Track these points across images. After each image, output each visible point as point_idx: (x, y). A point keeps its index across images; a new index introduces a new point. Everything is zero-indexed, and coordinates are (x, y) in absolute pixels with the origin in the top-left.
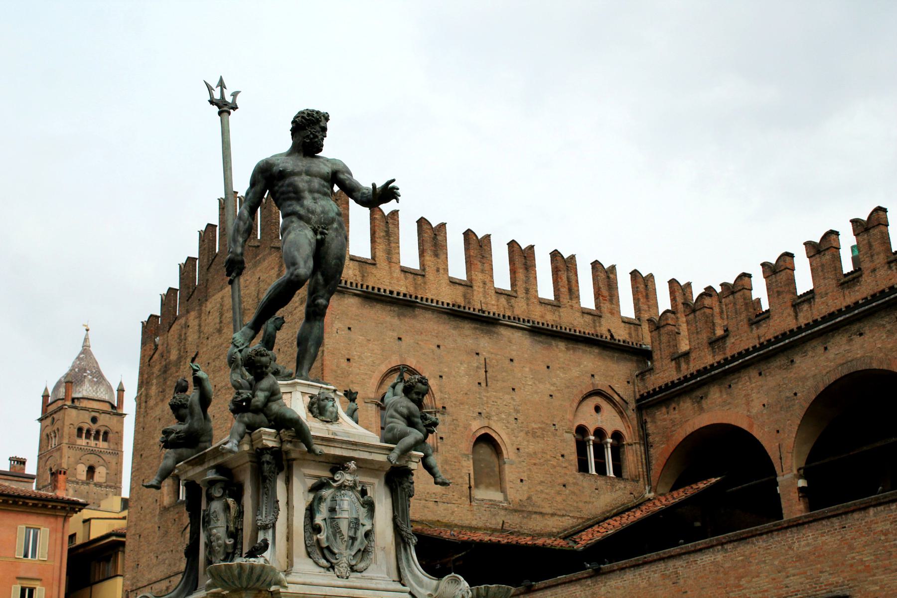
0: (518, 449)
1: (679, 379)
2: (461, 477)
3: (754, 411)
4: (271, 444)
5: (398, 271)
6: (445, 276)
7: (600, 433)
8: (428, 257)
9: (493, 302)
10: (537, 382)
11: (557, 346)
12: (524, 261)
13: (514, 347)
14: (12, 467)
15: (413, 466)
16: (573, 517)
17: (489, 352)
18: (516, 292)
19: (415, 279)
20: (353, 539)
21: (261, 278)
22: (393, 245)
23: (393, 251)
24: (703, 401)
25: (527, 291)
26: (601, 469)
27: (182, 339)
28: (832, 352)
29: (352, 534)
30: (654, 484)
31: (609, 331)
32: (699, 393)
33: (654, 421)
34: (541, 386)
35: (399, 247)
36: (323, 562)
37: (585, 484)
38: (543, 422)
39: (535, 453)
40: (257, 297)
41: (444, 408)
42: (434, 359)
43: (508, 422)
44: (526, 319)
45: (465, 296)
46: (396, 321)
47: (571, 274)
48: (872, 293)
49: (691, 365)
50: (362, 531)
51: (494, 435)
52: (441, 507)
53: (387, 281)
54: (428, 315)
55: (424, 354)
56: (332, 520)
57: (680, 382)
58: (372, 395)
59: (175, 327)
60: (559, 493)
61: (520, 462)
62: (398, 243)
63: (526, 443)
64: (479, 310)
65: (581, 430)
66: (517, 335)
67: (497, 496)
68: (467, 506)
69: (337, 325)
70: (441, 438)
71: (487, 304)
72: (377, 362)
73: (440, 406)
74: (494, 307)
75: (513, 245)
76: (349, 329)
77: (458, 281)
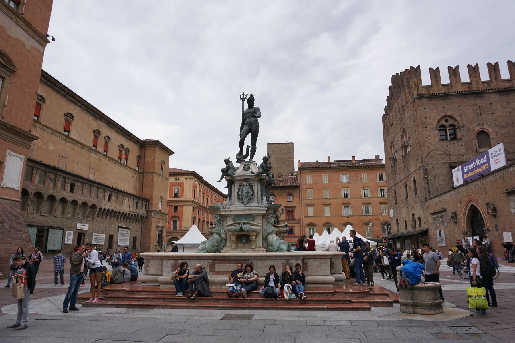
0: (496, 133)
2: (473, 146)
4: (228, 179)
5: (441, 86)
9: (481, 86)
10: (503, 109)
13: (492, 99)
14: (376, 158)
15: (264, 178)
19: (448, 87)
20: (247, 196)
22: (438, 78)
23: (439, 80)
25: (496, 79)
27: (389, 120)
29: (246, 195)
34: (505, 110)
35: (440, 78)
36: (241, 202)
38: (507, 122)
39: (504, 133)
41: (463, 125)
42: (458, 111)
43: (491, 125)
44: (497, 88)
45: (469, 87)
46: (442, 102)
50: (250, 195)
51: (485, 130)
56: (242, 193)
58: (436, 127)
59: (388, 117)
61: (497, 137)
62: (440, 77)
63: (500, 130)
64: (475, 91)
66: (493, 95)
69: (420, 108)
70: (463, 135)
71: (478, 87)
72: (436, 116)
73: (461, 125)
76: (425, 108)
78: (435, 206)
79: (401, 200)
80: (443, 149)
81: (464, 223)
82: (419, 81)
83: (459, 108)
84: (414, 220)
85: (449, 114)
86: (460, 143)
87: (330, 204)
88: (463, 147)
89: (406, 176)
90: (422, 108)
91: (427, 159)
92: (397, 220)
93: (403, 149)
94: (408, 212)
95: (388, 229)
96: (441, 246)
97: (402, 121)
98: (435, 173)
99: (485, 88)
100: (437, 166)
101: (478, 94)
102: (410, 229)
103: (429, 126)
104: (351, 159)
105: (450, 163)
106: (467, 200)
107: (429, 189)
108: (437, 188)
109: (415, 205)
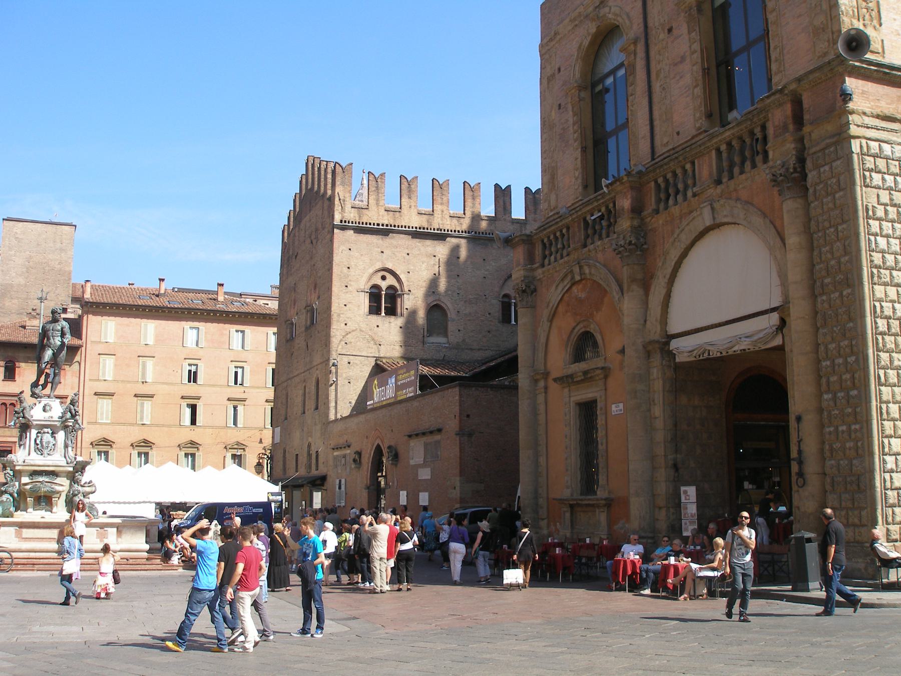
6: (416, 210)
9: (448, 223)
11: (492, 246)
12: (471, 193)
19: (394, 215)
22: (380, 195)
39: (470, 314)
41: (409, 291)
42: (404, 262)
45: (428, 221)
46: (380, 242)
47: (507, 199)
51: (442, 304)
53: (375, 218)
55: (398, 260)
58: (363, 287)
61: (459, 320)
63: (464, 308)
64: (438, 230)
67: (441, 340)
69: (342, 247)
71: (443, 224)
72: (367, 267)
76: (350, 249)
77: (423, 212)
78: (339, 436)
79: (295, 413)
80: (371, 330)
81: (367, 473)
82: (347, 195)
84: (309, 455)
85: (390, 266)
87: (152, 396)
90: (344, 248)
91: (340, 347)
92: (285, 452)
93: (309, 314)
95: (269, 465)
98: (351, 373)
99: (454, 227)
100: (356, 362)
102: (302, 472)
103: (352, 283)
104: (214, 288)
105: (377, 359)
107: (336, 403)
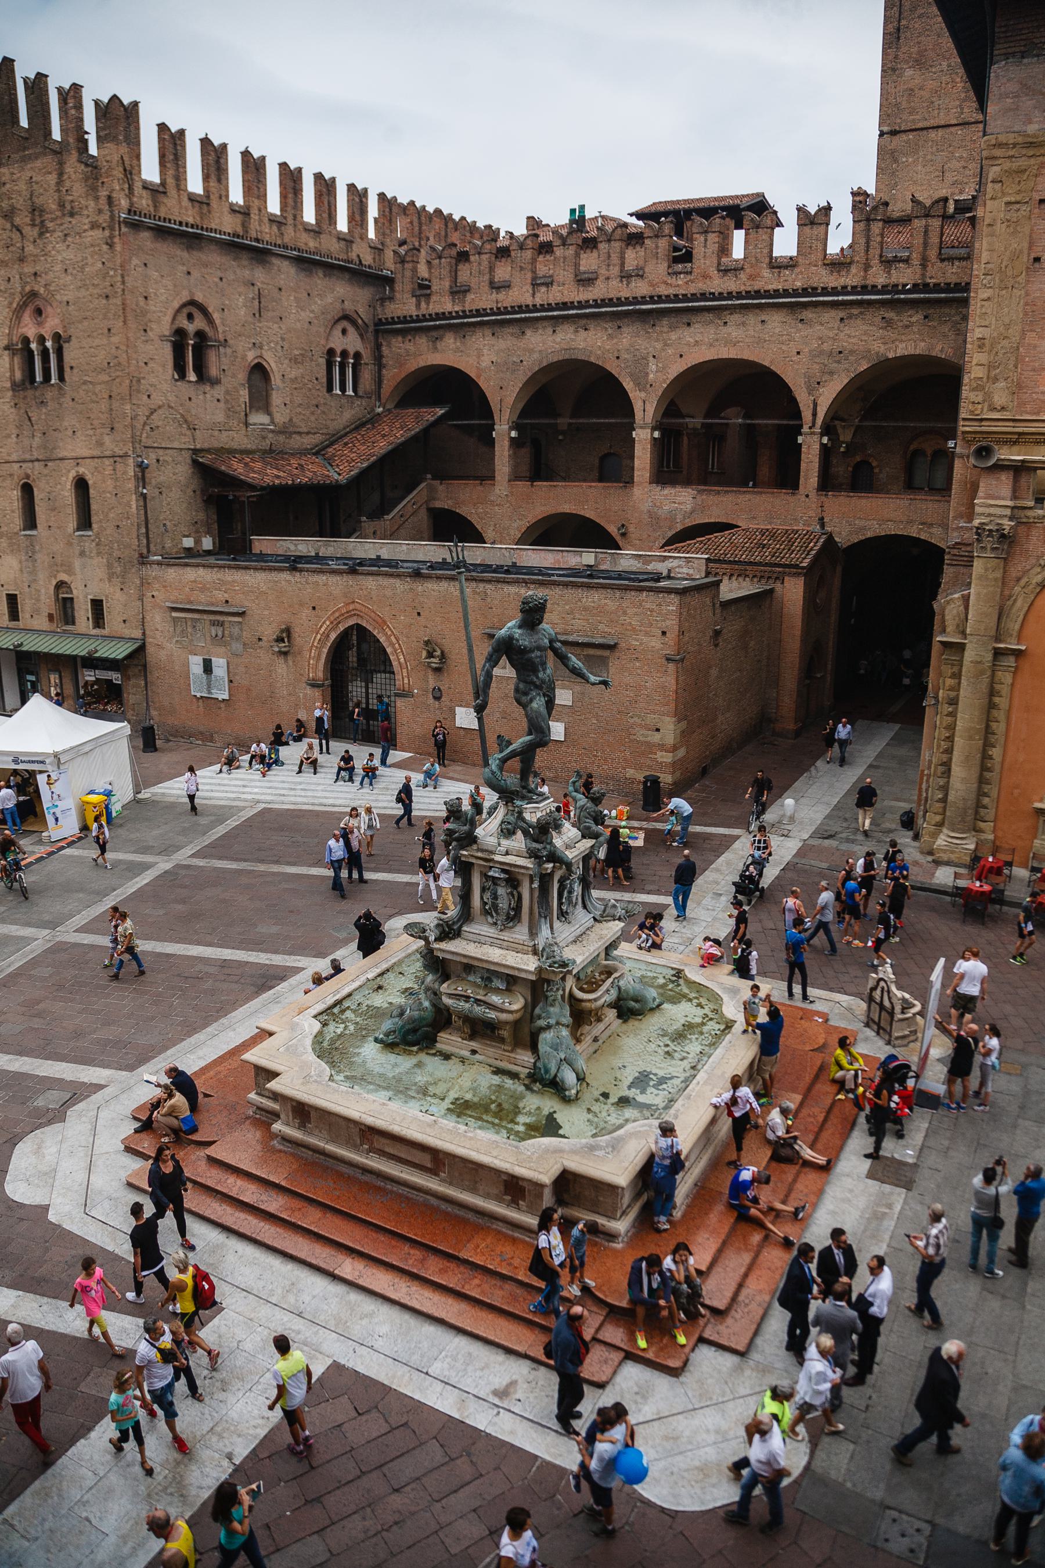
1: (417, 316)
3: (484, 364)
5: (186, 199)
7: (344, 354)
8: (213, 183)
16: (322, 434)
17: (263, 283)
18: (285, 218)
21: (34, 179)
22: (181, 170)
24: (438, 343)
25: (295, 217)
26: (343, 389)
28: (560, 336)
30: (383, 401)
31: (358, 256)
32: (435, 334)
33: (389, 345)
34: (302, 314)
37: (333, 404)
38: (303, 349)
40: (31, 199)
45: (244, 225)
46: (185, 254)
47: (332, 199)
48: (602, 297)
49: (431, 307)
51: (264, 363)
52: (225, 434)
53: (176, 210)
54: (213, 247)
57: (418, 321)
58: (167, 333)
60: (313, 413)
61: (284, 388)
62: (185, 167)
65: (331, 352)
66: (285, 264)
68: (244, 432)
69: (135, 261)
71: (261, 232)
73: (221, 338)
74: (269, 234)
75: (283, 166)
78: (192, 590)
80: (181, 405)
82: (135, 162)
83: (220, 284)
85: (199, 297)
86: (218, 392)
88: (222, 405)
89: (28, 457)
91: (144, 435)
94: (33, 572)
96: (202, 697)
97: (22, 260)
100: (166, 458)
101: (260, 254)
105: (195, 451)
106: (344, 611)
107: (147, 528)
108: (164, 525)
109: (77, 563)
